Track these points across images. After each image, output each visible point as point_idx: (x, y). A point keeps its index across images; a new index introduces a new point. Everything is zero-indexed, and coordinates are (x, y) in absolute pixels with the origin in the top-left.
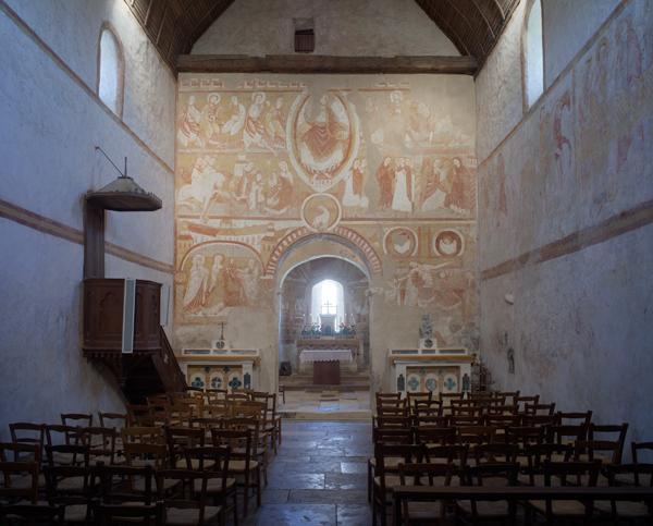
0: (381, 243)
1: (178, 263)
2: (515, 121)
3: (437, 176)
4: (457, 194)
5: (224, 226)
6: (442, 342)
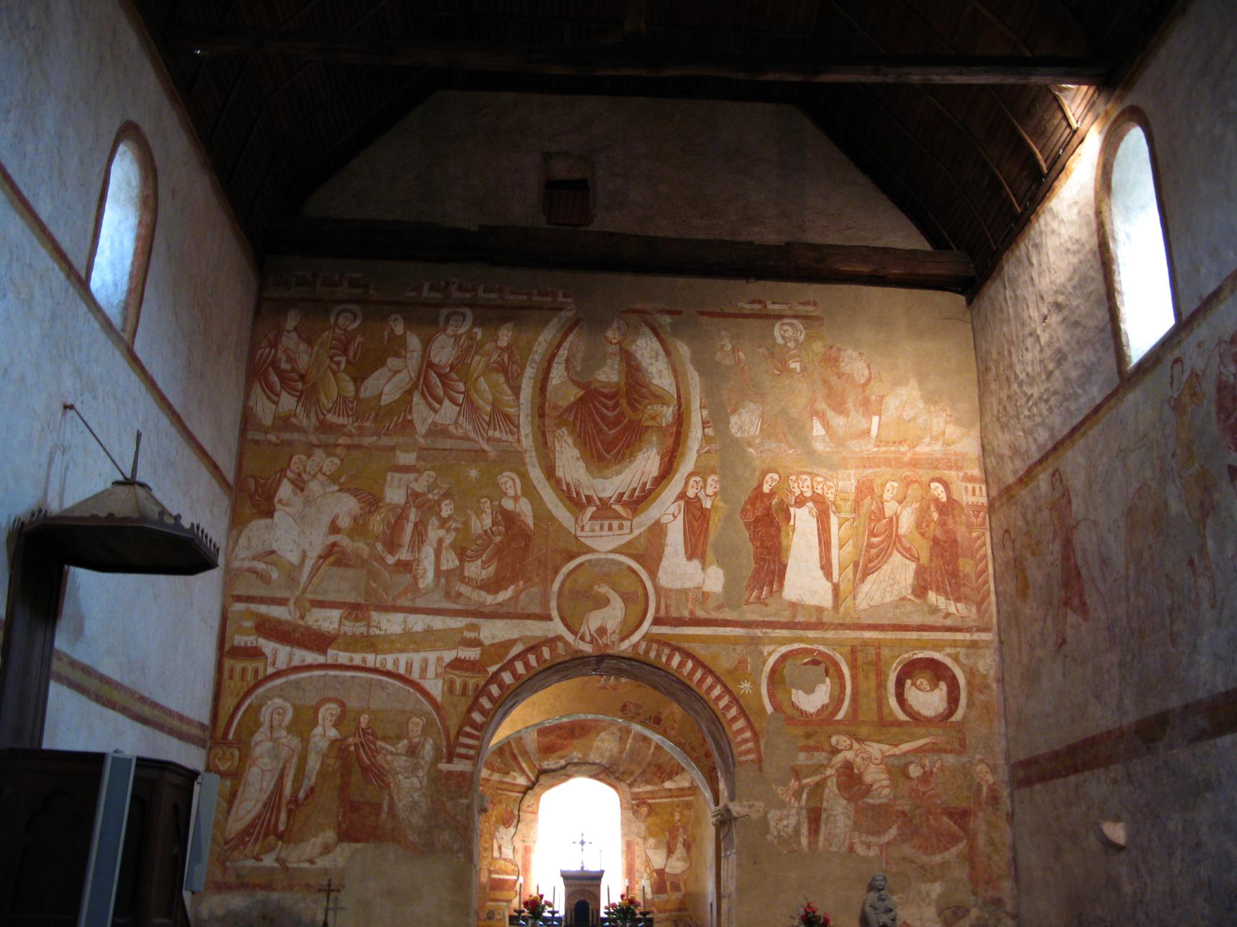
0: (756, 684)
1: (222, 725)
2: (1096, 393)
3: (894, 521)
4: (942, 567)
5: (350, 628)
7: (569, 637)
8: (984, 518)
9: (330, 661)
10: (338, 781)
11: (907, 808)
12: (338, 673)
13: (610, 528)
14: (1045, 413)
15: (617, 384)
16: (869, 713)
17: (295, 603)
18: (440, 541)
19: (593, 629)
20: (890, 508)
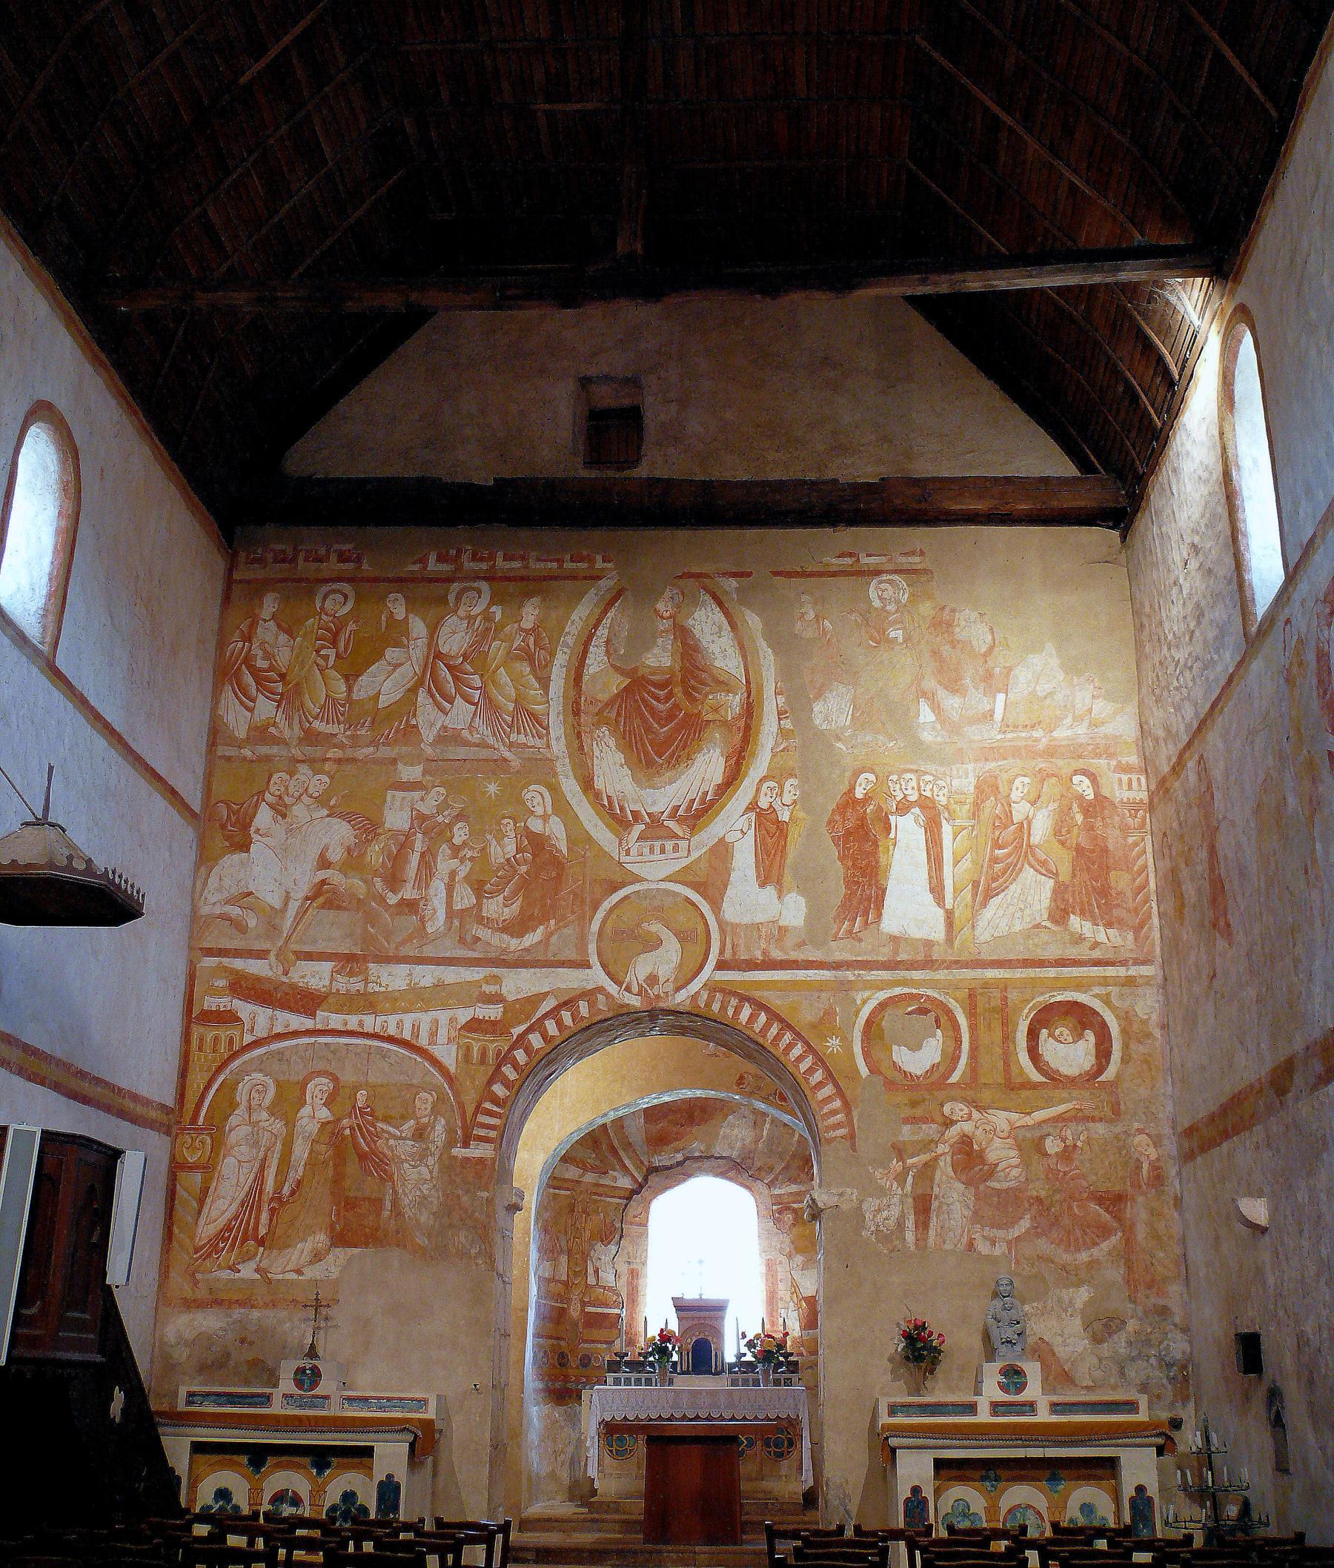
2: (1228, 659)
3: (1024, 827)
5: (345, 984)
6: (1058, 1375)
7: (612, 988)
8: (1144, 818)
9: (319, 1027)
10: (331, 1173)
11: (1043, 1194)
12: (329, 1040)
13: (663, 851)
14: (1190, 684)
15: (671, 668)
16: (992, 1071)
17: (277, 956)
18: (453, 874)
19: (641, 977)
20: (1020, 811)
